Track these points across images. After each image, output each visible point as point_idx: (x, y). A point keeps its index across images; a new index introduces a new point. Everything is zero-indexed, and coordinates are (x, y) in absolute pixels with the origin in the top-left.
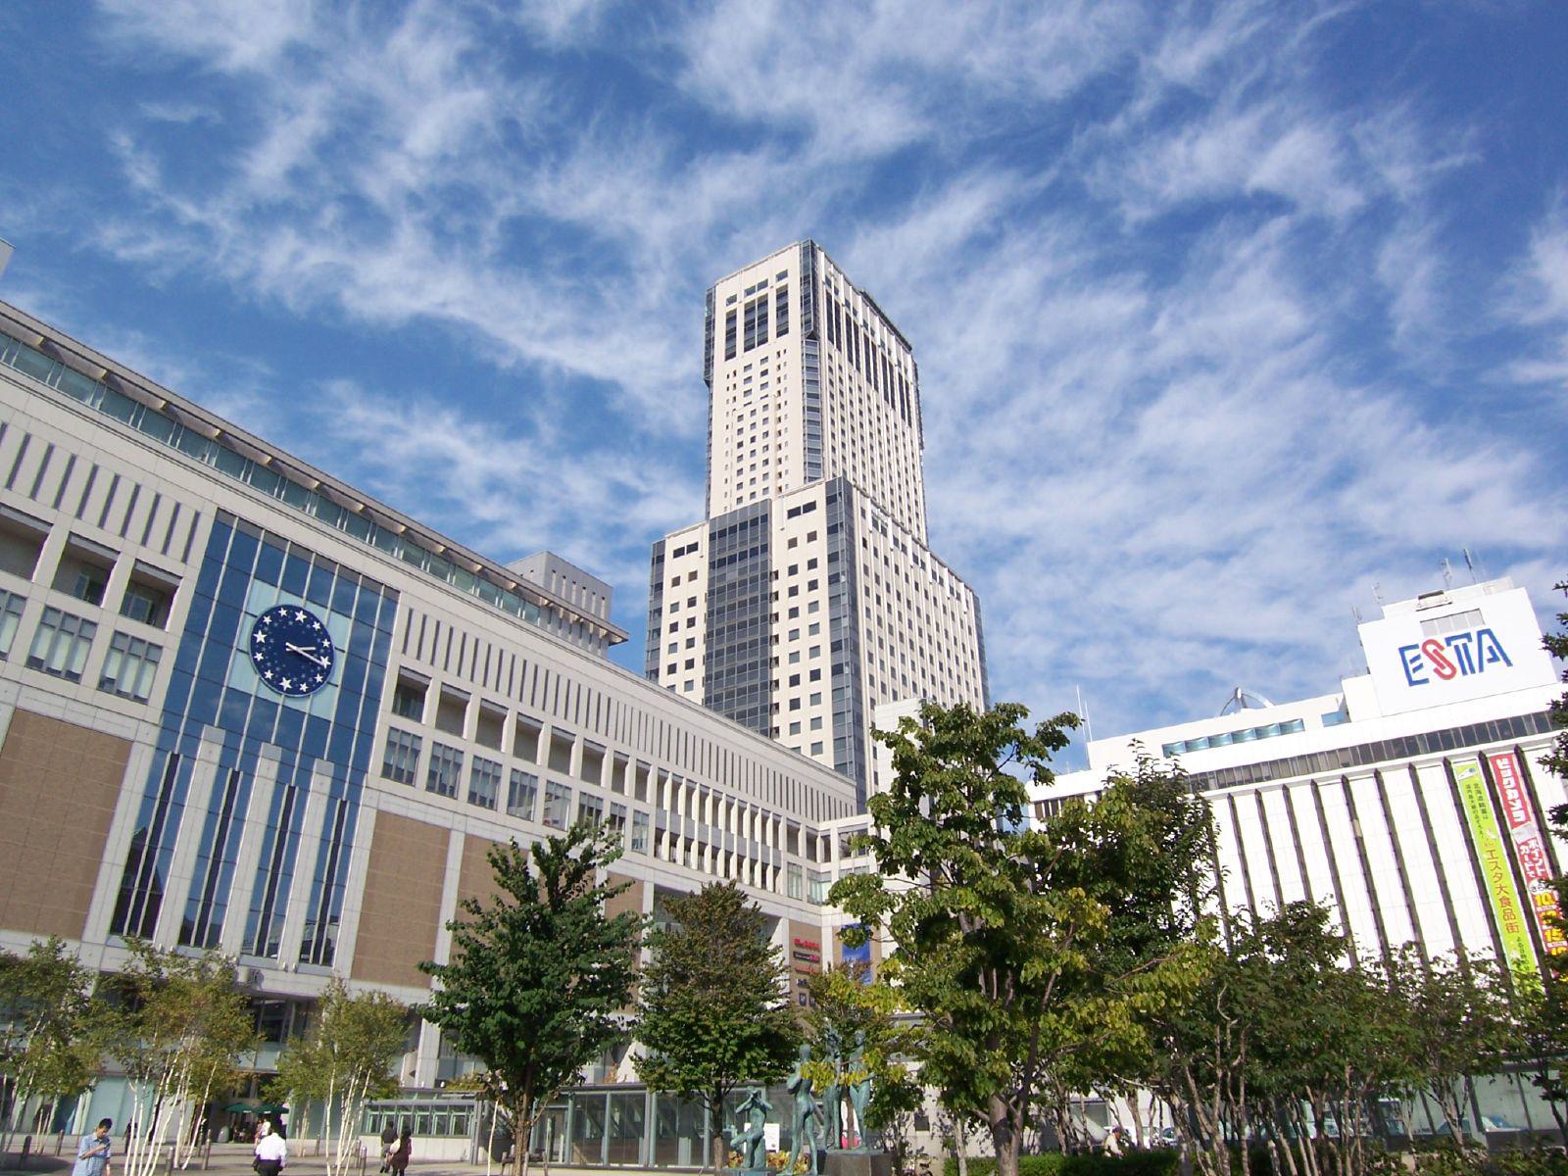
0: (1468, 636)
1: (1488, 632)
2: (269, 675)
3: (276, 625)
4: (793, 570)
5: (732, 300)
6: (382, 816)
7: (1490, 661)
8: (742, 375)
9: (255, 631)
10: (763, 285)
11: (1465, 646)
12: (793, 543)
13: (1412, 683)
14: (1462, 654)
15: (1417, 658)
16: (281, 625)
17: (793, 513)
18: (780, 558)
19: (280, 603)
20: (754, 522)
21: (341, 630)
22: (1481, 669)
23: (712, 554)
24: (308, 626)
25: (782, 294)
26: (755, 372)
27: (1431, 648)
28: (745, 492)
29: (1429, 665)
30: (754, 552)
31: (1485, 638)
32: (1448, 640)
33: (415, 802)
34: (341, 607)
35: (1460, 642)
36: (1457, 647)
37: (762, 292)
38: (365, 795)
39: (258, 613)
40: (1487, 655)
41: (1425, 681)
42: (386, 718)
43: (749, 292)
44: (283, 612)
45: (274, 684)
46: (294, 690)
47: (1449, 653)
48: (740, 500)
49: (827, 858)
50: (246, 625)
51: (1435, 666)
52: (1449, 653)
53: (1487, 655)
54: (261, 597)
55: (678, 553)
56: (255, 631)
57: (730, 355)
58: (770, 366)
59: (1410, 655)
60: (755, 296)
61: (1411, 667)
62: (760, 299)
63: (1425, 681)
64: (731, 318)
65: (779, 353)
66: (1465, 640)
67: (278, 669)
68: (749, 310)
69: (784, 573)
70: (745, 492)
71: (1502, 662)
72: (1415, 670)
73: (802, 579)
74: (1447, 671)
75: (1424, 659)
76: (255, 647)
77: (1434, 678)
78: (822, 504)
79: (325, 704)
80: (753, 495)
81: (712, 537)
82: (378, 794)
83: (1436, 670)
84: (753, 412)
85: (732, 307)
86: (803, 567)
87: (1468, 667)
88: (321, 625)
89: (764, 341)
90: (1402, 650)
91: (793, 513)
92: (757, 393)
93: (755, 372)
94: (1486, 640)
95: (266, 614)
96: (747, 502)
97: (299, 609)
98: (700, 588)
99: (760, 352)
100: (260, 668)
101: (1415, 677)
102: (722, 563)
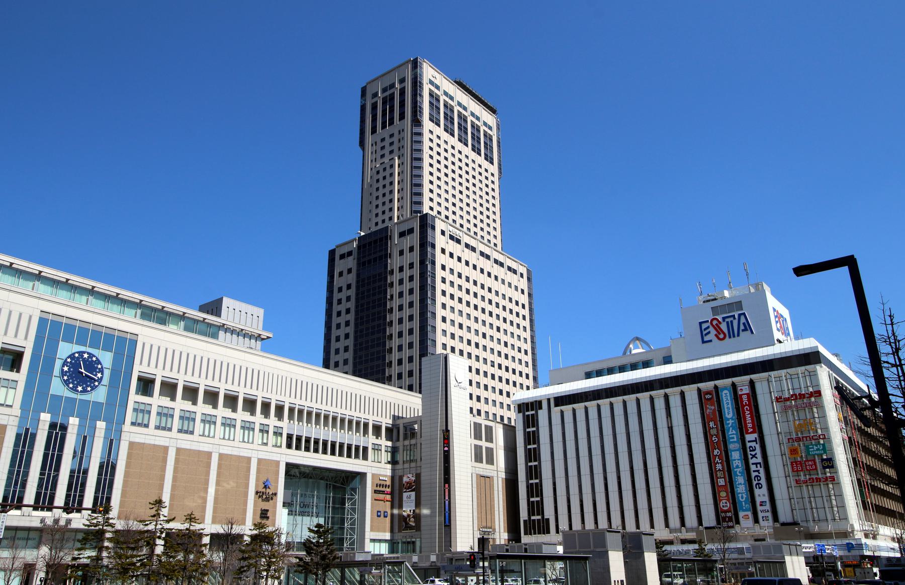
0: (734, 316)
1: (744, 314)
2: (71, 386)
3: (73, 361)
6: (132, 445)
7: (743, 330)
9: (63, 366)
11: (732, 322)
13: (704, 342)
14: (730, 326)
15: (708, 327)
16: (76, 361)
17: (402, 235)
18: (394, 262)
19: (73, 352)
21: (106, 359)
22: (738, 335)
23: (359, 259)
24: (90, 360)
25: (402, 92)
26: (386, 143)
27: (715, 322)
28: (379, 219)
29: (713, 332)
30: (381, 258)
31: (742, 318)
32: (724, 319)
33: (150, 436)
34: (107, 348)
35: (729, 320)
36: (727, 322)
38: (124, 436)
39: (64, 358)
40: (742, 327)
41: (711, 341)
42: (134, 397)
44: (77, 355)
45: (74, 389)
46: (84, 391)
47: (724, 327)
48: (377, 224)
49: (398, 440)
50: (58, 364)
51: (715, 332)
52: (724, 327)
53: (742, 327)
54: (65, 350)
55: (342, 257)
56: (63, 366)
57: (374, 131)
59: (704, 326)
60: (387, 93)
61: (704, 333)
63: (711, 341)
64: (374, 107)
66: (732, 319)
67: (76, 382)
71: (749, 331)
72: (706, 334)
74: (721, 336)
75: (711, 329)
76: (63, 373)
77: (715, 339)
79: (100, 395)
80: (383, 221)
82: (131, 434)
83: (716, 335)
84: (385, 169)
87: (732, 334)
88: (97, 358)
90: (701, 323)
91: (402, 235)
93: (386, 143)
94: (743, 320)
95: (68, 357)
97: (84, 352)
98: (352, 278)
100: (66, 383)
101: (706, 339)
102: (364, 264)
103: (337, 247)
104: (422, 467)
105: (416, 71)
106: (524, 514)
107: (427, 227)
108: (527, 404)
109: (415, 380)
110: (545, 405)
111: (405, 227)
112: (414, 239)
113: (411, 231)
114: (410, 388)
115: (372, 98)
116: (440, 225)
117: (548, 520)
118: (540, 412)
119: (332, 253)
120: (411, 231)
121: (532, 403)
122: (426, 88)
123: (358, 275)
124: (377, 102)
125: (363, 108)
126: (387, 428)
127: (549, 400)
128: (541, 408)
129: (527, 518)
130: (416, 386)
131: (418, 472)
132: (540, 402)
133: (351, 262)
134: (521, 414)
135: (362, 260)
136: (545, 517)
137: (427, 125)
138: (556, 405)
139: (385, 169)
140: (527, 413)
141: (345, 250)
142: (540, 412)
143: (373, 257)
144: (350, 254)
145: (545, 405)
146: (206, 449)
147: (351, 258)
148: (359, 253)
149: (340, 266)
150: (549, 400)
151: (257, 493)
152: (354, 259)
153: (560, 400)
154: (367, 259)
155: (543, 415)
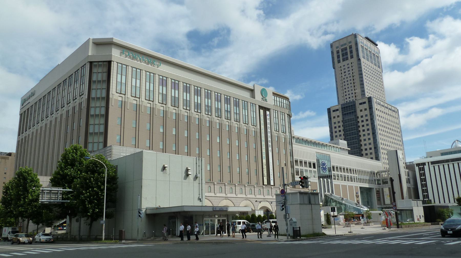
5: (337, 47)
8: (343, 68)
10: (345, 44)
12: (361, 111)
17: (361, 104)
18: (359, 114)
20: (352, 106)
23: (342, 113)
25: (351, 47)
30: (353, 112)
43: (342, 46)
55: (334, 111)
57: (339, 62)
58: (350, 66)
62: (345, 48)
64: (338, 52)
65: (351, 63)
69: (360, 117)
70: (348, 97)
73: (364, 119)
80: (349, 98)
81: (342, 108)
85: (338, 49)
86: (364, 116)
89: (347, 59)
91: (361, 104)
92: (347, 73)
98: (340, 119)
99: (347, 62)
102: (345, 114)
103: (331, 107)
105: (356, 39)
107: (372, 101)
108: (420, 164)
109: (373, 156)
110: (427, 164)
111: (361, 101)
112: (366, 106)
113: (365, 103)
114: (372, 158)
115: (336, 49)
117: (431, 200)
119: (329, 110)
120: (365, 103)
121: (421, 163)
122: (360, 45)
123: (343, 118)
125: (332, 53)
126: (376, 173)
127: (428, 163)
128: (425, 165)
130: (374, 158)
132: (425, 163)
133: (339, 113)
134: (418, 167)
137: (362, 60)
143: (349, 112)
144: (337, 110)
145: (427, 164)
147: (338, 112)
148: (342, 110)
149: (333, 114)
150: (428, 163)
151: (356, 196)
152: (340, 112)
153: (433, 163)
154: (346, 112)
155: (426, 167)
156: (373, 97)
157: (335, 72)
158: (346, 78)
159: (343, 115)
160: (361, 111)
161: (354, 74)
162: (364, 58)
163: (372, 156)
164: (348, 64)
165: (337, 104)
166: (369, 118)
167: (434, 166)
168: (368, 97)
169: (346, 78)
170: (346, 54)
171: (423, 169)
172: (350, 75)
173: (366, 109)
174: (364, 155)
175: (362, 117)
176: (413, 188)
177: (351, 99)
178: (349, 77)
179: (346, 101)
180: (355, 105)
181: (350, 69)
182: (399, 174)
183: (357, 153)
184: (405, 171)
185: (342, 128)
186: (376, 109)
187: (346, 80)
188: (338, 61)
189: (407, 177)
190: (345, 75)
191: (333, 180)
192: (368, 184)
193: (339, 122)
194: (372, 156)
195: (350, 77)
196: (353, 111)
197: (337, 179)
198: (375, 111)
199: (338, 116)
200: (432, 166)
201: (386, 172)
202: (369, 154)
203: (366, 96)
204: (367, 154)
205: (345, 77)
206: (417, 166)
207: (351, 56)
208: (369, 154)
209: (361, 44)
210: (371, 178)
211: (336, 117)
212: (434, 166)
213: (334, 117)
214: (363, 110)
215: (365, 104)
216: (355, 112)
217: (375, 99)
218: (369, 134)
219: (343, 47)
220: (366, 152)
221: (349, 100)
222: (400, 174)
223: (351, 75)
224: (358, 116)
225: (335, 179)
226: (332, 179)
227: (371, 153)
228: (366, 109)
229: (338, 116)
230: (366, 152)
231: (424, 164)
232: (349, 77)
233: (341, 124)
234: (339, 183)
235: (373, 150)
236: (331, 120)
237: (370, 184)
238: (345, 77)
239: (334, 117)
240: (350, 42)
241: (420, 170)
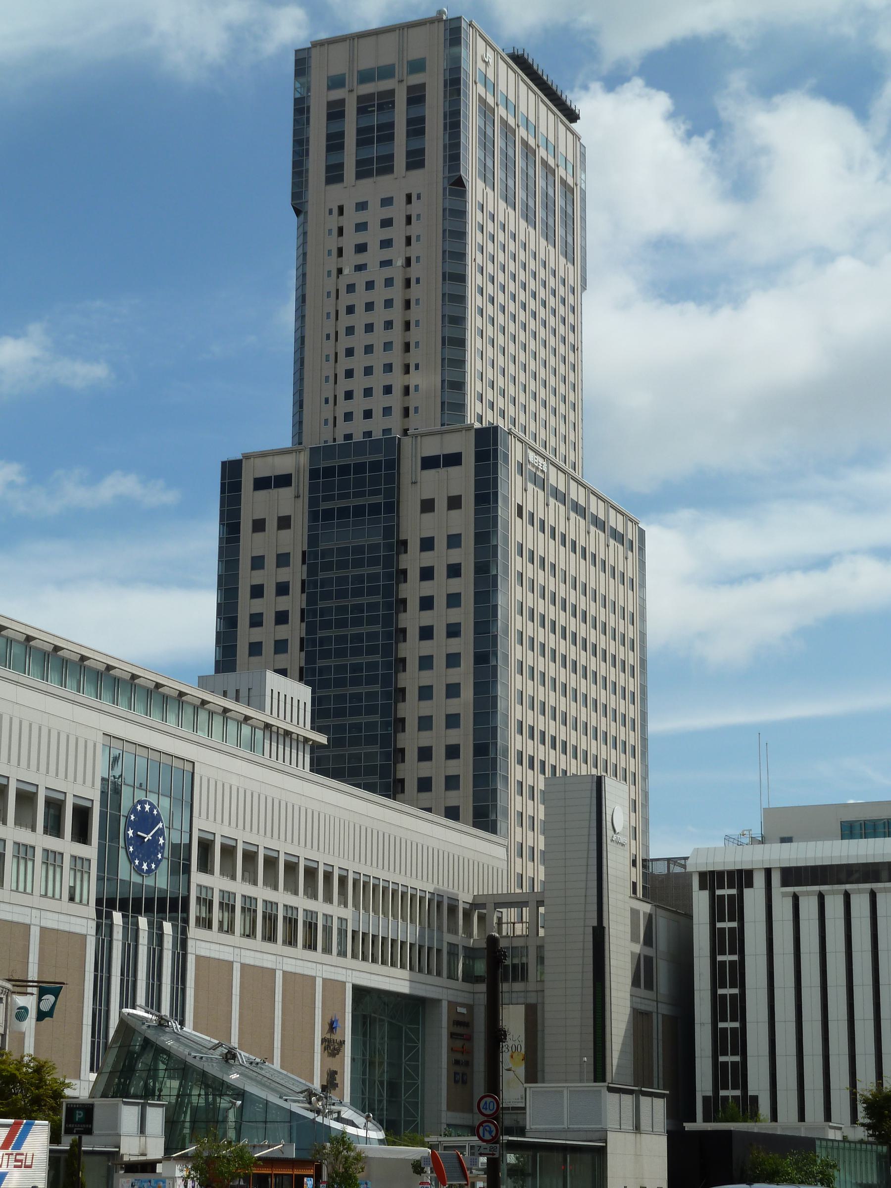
4: (427, 544)
5: (336, 82)
8: (351, 218)
10: (386, 72)
12: (428, 506)
17: (429, 463)
23: (313, 502)
25: (416, 96)
30: (375, 509)
37: (384, 85)
43: (365, 77)
55: (262, 484)
57: (334, 174)
58: (397, 211)
64: (335, 112)
68: (364, 106)
69: (414, 545)
78: (469, 459)
81: (314, 474)
84: (370, 285)
86: (441, 543)
89: (386, 166)
91: (429, 463)
96: (358, 428)
99: (381, 186)
102: (328, 514)
103: (247, 457)
104: (547, 993)
105: (454, 50)
106: (704, 1084)
107: (496, 458)
108: (721, 874)
109: (464, 798)
110: (759, 880)
111: (432, 448)
113: (454, 460)
114: (452, 813)
116: (516, 452)
117: (755, 1099)
118: (747, 892)
120: (454, 460)
121: (731, 873)
123: (313, 540)
124: (342, 102)
125: (301, 109)
127: (768, 872)
128: (750, 885)
129: (710, 1094)
130: (467, 810)
131: (532, 1000)
135: (324, 506)
136: (750, 1093)
138: (785, 883)
139: (370, 285)
140: (719, 892)
141: (264, 469)
142: (747, 892)
143: (352, 502)
144: (284, 481)
145: (759, 880)
146: (21, 920)
147: (286, 493)
148: (313, 488)
150: (768, 872)
152: (297, 497)
155: (754, 899)
156: (510, 433)
157: (303, 235)
158: (360, 287)
159: (314, 516)
160: (428, 506)
161: (415, 271)
162: (486, 175)
163: (453, 798)
164: (387, 202)
165: (287, 442)
166: (465, 555)
167: (796, 898)
168: (477, 425)
169: (360, 287)
170: (386, 133)
171: (736, 910)
172: (387, 272)
173: (454, 503)
174: (411, 785)
175: (427, 544)
176: (663, 1015)
177: (377, 426)
178: (379, 284)
179: (343, 428)
180: (393, 464)
181: (397, 233)
182: (595, 924)
183: (370, 771)
184: (634, 913)
185: (294, 603)
186: (514, 510)
187: (360, 298)
188: (329, 168)
189: (637, 948)
190: (360, 268)
191: (193, 931)
192: (405, 974)
193: (283, 560)
194: (453, 798)
195: (389, 282)
196: (379, 499)
197: (221, 923)
198: (506, 523)
199: (284, 523)
200: (784, 895)
201: (525, 904)
202: (439, 784)
203: (471, 419)
204: (425, 785)
205: (360, 279)
206: (702, 887)
207: (409, 154)
208: (439, 784)
209: (481, 89)
210: (431, 938)
211: (272, 524)
212: (796, 898)
213: (259, 526)
214: (441, 504)
215: (453, 471)
216: (392, 507)
217: (519, 445)
218: (453, 660)
219: (367, 89)
220: (425, 769)
221: (368, 425)
222: (605, 924)
223: (396, 272)
224: (402, 537)
225: (205, 923)
226: (186, 921)
227: (452, 782)
228: (454, 503)
229: (284, 523)
230: (425, 769)
231: (743, 878)
232: (379, 284)
233: (295, 573)
234: (225, 954)
235: (464, 767)
236: (238, 540)
237: (420, 971)
238: (360, 279)
239: (259, 526)
240: (417, 66)
241: (717, 910)
